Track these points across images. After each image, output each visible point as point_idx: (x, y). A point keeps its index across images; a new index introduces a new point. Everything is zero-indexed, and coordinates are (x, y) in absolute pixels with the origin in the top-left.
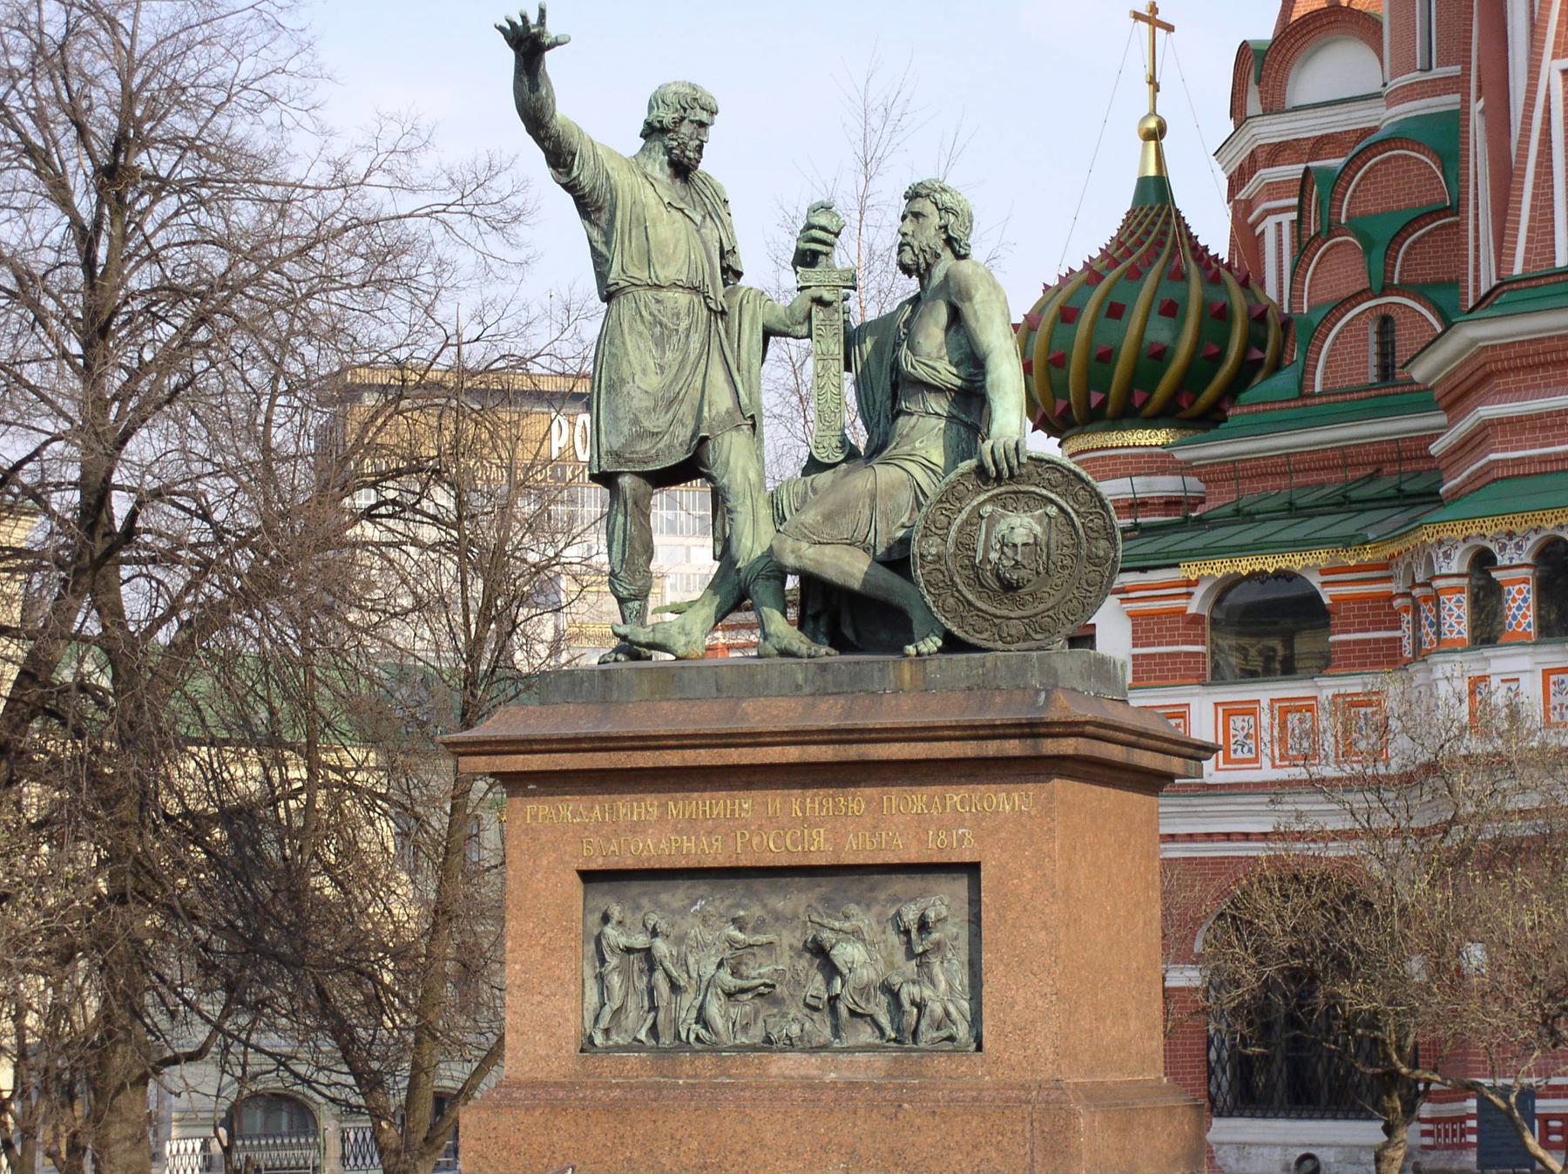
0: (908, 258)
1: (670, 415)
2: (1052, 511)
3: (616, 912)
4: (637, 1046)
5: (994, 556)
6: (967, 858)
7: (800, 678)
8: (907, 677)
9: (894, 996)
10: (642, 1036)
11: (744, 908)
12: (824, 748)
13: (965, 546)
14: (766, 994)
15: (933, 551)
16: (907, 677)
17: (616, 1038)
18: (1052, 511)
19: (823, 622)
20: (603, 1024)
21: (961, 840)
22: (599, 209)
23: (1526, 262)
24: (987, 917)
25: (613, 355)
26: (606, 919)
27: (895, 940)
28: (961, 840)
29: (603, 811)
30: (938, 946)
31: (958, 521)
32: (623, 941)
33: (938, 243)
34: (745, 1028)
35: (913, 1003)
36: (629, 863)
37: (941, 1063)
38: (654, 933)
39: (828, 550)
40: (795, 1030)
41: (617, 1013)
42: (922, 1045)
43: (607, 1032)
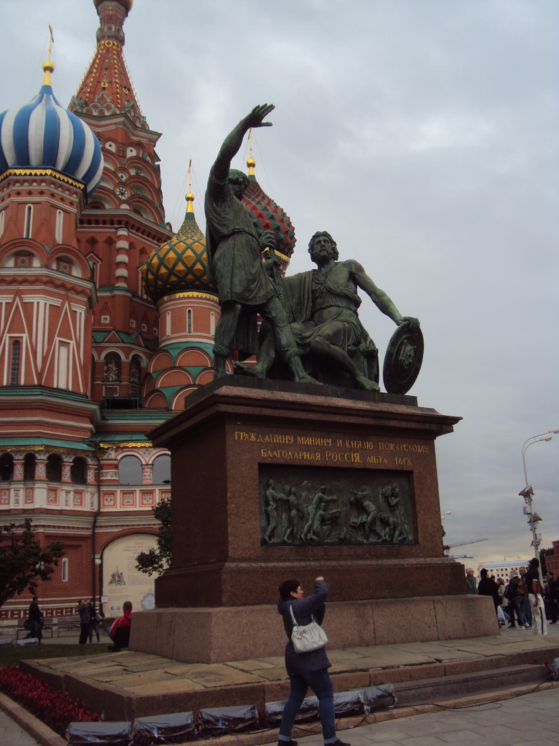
0: (324, 253)
1: (255, 285)
3: (271, 481)
4: (284, 543)
5: (404, 358)
7: (339, 393)
8: (377, 398)
9: (385, 523)
10: (286, 538)
11: (324, 485)
12: (370, 419)
13: (398, 353)
14: (334, 521)
15: (392, 351)
16: (377, 398)
17: (273, 540)
20: (267, 533)
21: (406, 463)
22: (224, 201)
24: (417, 492)
25: (240, 255)
27: (381, 499)
28: (406, 463)
29: (269, 437)
30: (397, 504)
31: (399, 343)
36: (282, 461)
38: (290, 493)
40: (348, 537)
43: (270, 537)
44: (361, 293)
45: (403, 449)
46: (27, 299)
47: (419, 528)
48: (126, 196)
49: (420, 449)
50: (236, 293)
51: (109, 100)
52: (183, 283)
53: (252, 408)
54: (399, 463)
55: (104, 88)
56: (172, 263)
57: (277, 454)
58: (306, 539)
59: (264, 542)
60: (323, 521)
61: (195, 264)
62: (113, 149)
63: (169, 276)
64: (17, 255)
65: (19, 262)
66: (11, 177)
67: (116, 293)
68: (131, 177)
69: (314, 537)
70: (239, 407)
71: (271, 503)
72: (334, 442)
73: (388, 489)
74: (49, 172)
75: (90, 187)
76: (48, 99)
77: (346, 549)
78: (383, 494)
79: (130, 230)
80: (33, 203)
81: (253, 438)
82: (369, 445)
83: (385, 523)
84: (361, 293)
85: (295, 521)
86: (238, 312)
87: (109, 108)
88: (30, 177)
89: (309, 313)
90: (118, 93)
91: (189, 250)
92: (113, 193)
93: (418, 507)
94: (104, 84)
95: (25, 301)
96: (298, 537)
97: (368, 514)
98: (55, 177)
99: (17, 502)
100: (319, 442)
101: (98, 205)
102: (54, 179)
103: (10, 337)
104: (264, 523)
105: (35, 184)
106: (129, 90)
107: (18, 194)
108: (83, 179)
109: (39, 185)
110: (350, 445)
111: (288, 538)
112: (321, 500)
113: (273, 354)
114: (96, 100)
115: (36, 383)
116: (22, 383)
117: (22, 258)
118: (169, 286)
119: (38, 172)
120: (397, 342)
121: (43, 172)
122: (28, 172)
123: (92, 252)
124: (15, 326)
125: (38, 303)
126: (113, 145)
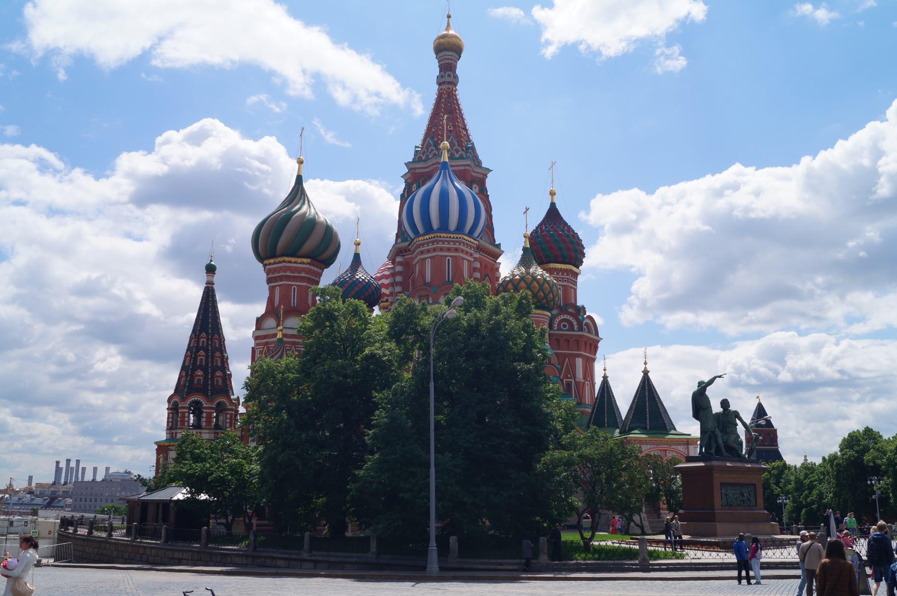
44: (738, 421)
61: (538, 292)
80: (451, 256)
84: (738, 421)
107: (441, 249)
119: (455, 236)
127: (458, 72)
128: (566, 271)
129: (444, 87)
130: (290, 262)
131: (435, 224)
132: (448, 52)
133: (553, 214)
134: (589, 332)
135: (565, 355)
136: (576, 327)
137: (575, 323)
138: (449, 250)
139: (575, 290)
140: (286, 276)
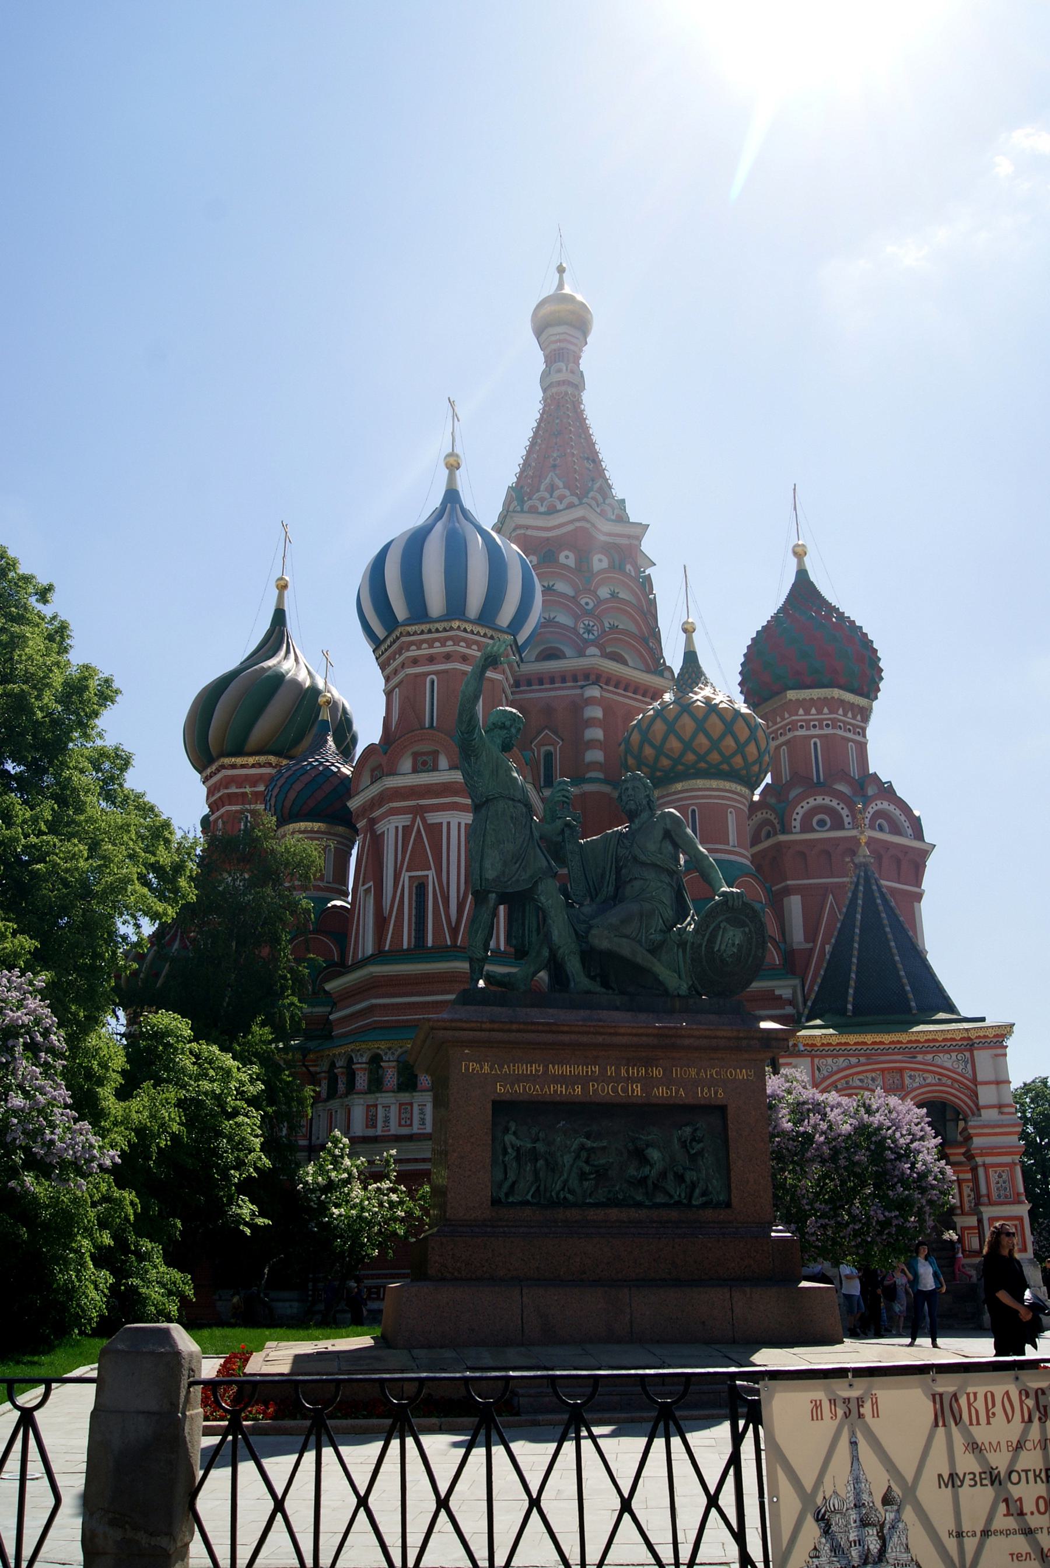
0: (632, 806)
2: (747, 930)
3: (513, 1126)
4: (527, 1203)
5: (723, 947)
6: (719, 1103)
9: (680, 1178)
10: (529, 1197)
13: (711, 941)
14: (601, 1174)
18: (747, 930)
19: (598, 979)
21: (716, 1093)
23: (390, 946)
24: (732, 1134)
26: (506, 1130)
27: (676, 1145)
28: (716, 1093)
29: (509, 1067)
30: (700, 1153)
32: (518, 1143)
33: (645, 802)
34: (590, 1196)
35: (692, 1183)
37: (709, 1214)
38: (536, 1140)
39: (624, 940)
41: (514, 1183)
42: (694, 1203)
43: (507, 1195)
45: (711, 1075)
46: (433, 818)
47: (733, 1185)
48: (596, 633)
49: (742, 1074)
50: (487, 880)
51: (561, 485)
52: (680, 767)
53: (478, 1033)
54: (704, 1094)
55: (554, 466)
56: (659, 737)
57: (519, 1088)
58: (558, 1197)
59: (495, 1202)
60: (583, 1176)
61: (694, 736)
62: (571, 562)
63: (657, 759)
64: (416, 755)
65: (419, 764)
66: (404, 639)
67: (588, 788)
68: (600, 602)
69: (569, 1196)
70: (462, 1032)
71: (510, 1150)
72: (603, 1070)
73: (688, 1130)
74: (455, 624)
75: (521, 639)
76: (453, 509)
77: (614, 1213)
78: (679, 1139)
79: (605, 687)
81: (486, 1068)
82: (657, 1072)
83: (680, 1178)
85: (542, 1174)
86: (492, 903)
87: (561, 498)
88: (430, 636)
89: (611, 889)
90: (575, 471)
91: (685, 714)
92: (575, 630)
93: (733, 1156)
94: (555, 460)
95: (429, 822)
96: (548, 1195)
97: (652, 1166)
98: (465, 630)
99: (423, 1122)
100: (580, 1070)
101: (551, 654)
102: (464, 634)
103: (410, 877)
104: (500, 1176)
105: (437, 644)
106: (594, 461)
107: (415, 661)
108: (508, 627)
109: (443, 645)
110: (627, 1071)
111: (532, 1196)
112: (582, 1147)
113: (546, 953)
114: (542, 487)
115: (449, 943)
116: (430, 944)
117: (425, 758)
118: (658, 774)
119: (439, 626)
120: (708, 927)
121: (445, 625)
122: (425, 627)
123: (546, 727)
124: (418, 861)
125: (449, 823)
126: (571, 555)
127: (584, 365)
128: (826, 702)
129: (554, 390)
130: (233, 766)
131: (400, 611)
132: (562, 329)
133: (803, 592)
134: (896, 830)
135: (825, 889)
136: (847, 820)
137: (845, 812)
138: (431, 659)
139: (862, 748)
140: (229, 796)
